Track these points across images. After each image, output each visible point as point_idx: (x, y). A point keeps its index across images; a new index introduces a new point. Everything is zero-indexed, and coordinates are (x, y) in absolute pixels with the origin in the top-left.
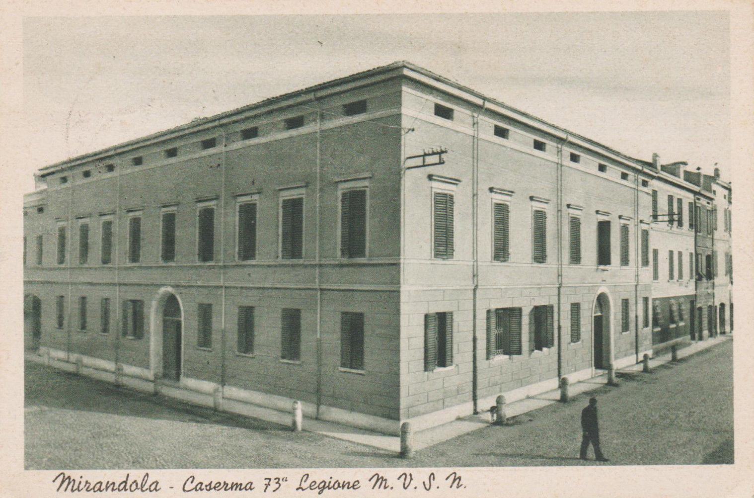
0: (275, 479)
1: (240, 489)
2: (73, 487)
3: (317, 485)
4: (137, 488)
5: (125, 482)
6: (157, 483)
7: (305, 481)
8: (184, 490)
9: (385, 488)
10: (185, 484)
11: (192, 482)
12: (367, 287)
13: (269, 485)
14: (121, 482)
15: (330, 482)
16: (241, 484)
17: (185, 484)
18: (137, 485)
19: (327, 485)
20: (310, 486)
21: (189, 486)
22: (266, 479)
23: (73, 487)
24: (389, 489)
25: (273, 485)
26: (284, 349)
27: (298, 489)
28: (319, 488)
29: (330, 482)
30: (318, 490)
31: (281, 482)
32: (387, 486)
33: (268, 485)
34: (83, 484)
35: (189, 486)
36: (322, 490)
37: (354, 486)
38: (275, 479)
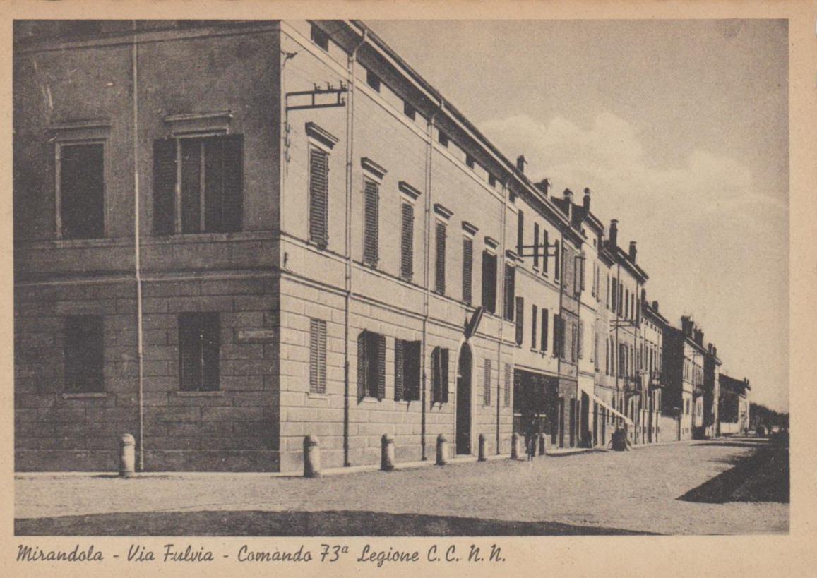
0: (334, 547)
1: (268, 560)
2: (29, 556)
3: (376, 557)
4: (253, 559)
5: (300, 553)
6: (347, 548)
7: (367, 552)
8: (240, 560)
9: (497, 560)
10: (239, 554)
11: (246, 552)
12: (500, 269)
13: (328, 553)
14: (429, 548)
15: (389, 553)
16: (268, 554)
17: (239, 554)
18: (253, 556)
19: (386, 556)
20: (371, 557)
21: (244, 555)
22: (323, 545)
23: (29, 556)
24: (501, 561)
25: (331, 555)
26: (447, 353)
27: (359, 560)
28: (378, 560)
29: (389, 553)
30: (376, 562)
31: (340, 553)
32: (499, 557)
33: (325, 554)
34: (38, 554)
35: (244, 555)
36: (382, 562)
37: (413, 557)
38: (334, 547)
